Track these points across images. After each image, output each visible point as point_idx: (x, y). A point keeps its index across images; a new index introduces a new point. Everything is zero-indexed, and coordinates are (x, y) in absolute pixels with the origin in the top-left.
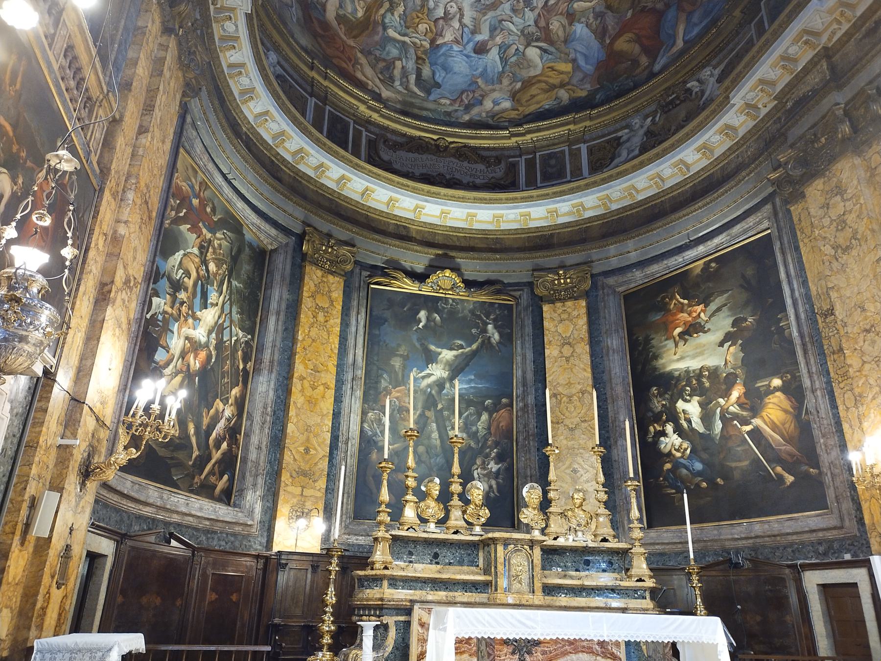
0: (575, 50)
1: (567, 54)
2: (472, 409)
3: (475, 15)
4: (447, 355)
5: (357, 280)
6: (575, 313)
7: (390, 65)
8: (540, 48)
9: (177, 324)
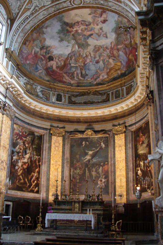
1: (119, 60)
3: (94, 53)
4: (91, 153)
6: (122, 138)
7: (73, 73)
8: (111, 59)
9: (19, 161)
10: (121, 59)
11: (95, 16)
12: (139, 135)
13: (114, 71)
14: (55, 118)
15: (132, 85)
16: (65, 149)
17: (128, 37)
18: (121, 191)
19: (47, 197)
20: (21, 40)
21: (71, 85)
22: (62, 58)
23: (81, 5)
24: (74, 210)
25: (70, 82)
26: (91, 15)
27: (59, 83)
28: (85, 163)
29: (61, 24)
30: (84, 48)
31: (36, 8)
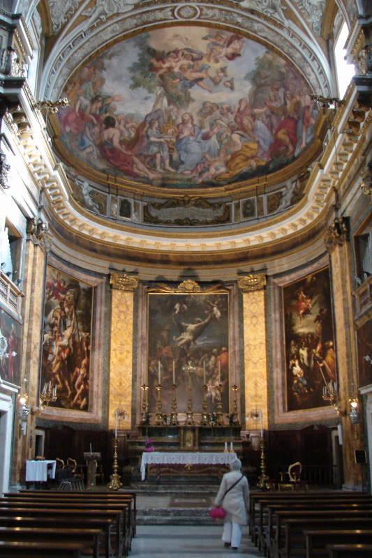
1: (254, 138)
3: (200, 119)
4: (192, 327)
6: (259, 299)
7: (153, 157)
8: (239, 134)
10: (259, 136)
12: (298, 296)
13: (242, 159)
14: (121, 253)
15: (281, 193)
17: (281, 93)
18: (256, 406)
19: (106, 419)
21: (149, 182)
22: (133, 124)
24: (184, 445)
25: (146, 176)
27: (125, 177)
28: (179, 348)
29: (140, 52)
30: (179, 106)
31: (102, 17)
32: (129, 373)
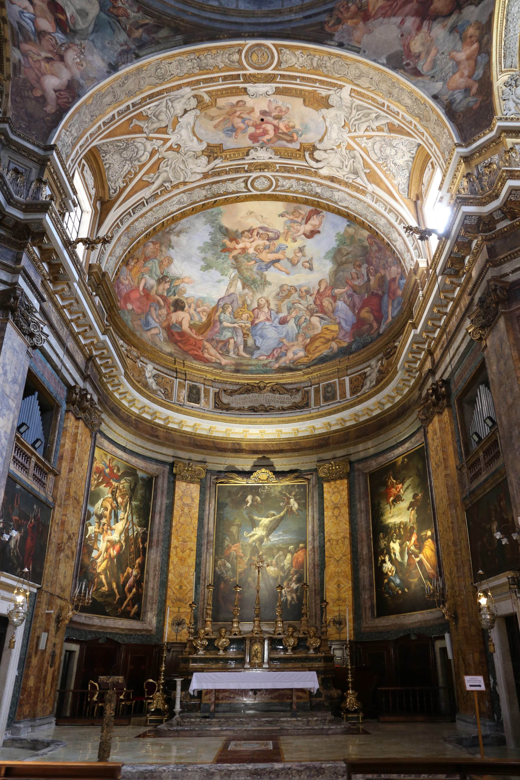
0: (339, 317)
2: (281, 553)
3: (277, 302)
5: (209, 482)
11: (293, 221)
16: (204, 511)
20: (121, 253)
23: (268, 192)
26: (283, 216)
27: (195, 362)
32: (191, 574)
